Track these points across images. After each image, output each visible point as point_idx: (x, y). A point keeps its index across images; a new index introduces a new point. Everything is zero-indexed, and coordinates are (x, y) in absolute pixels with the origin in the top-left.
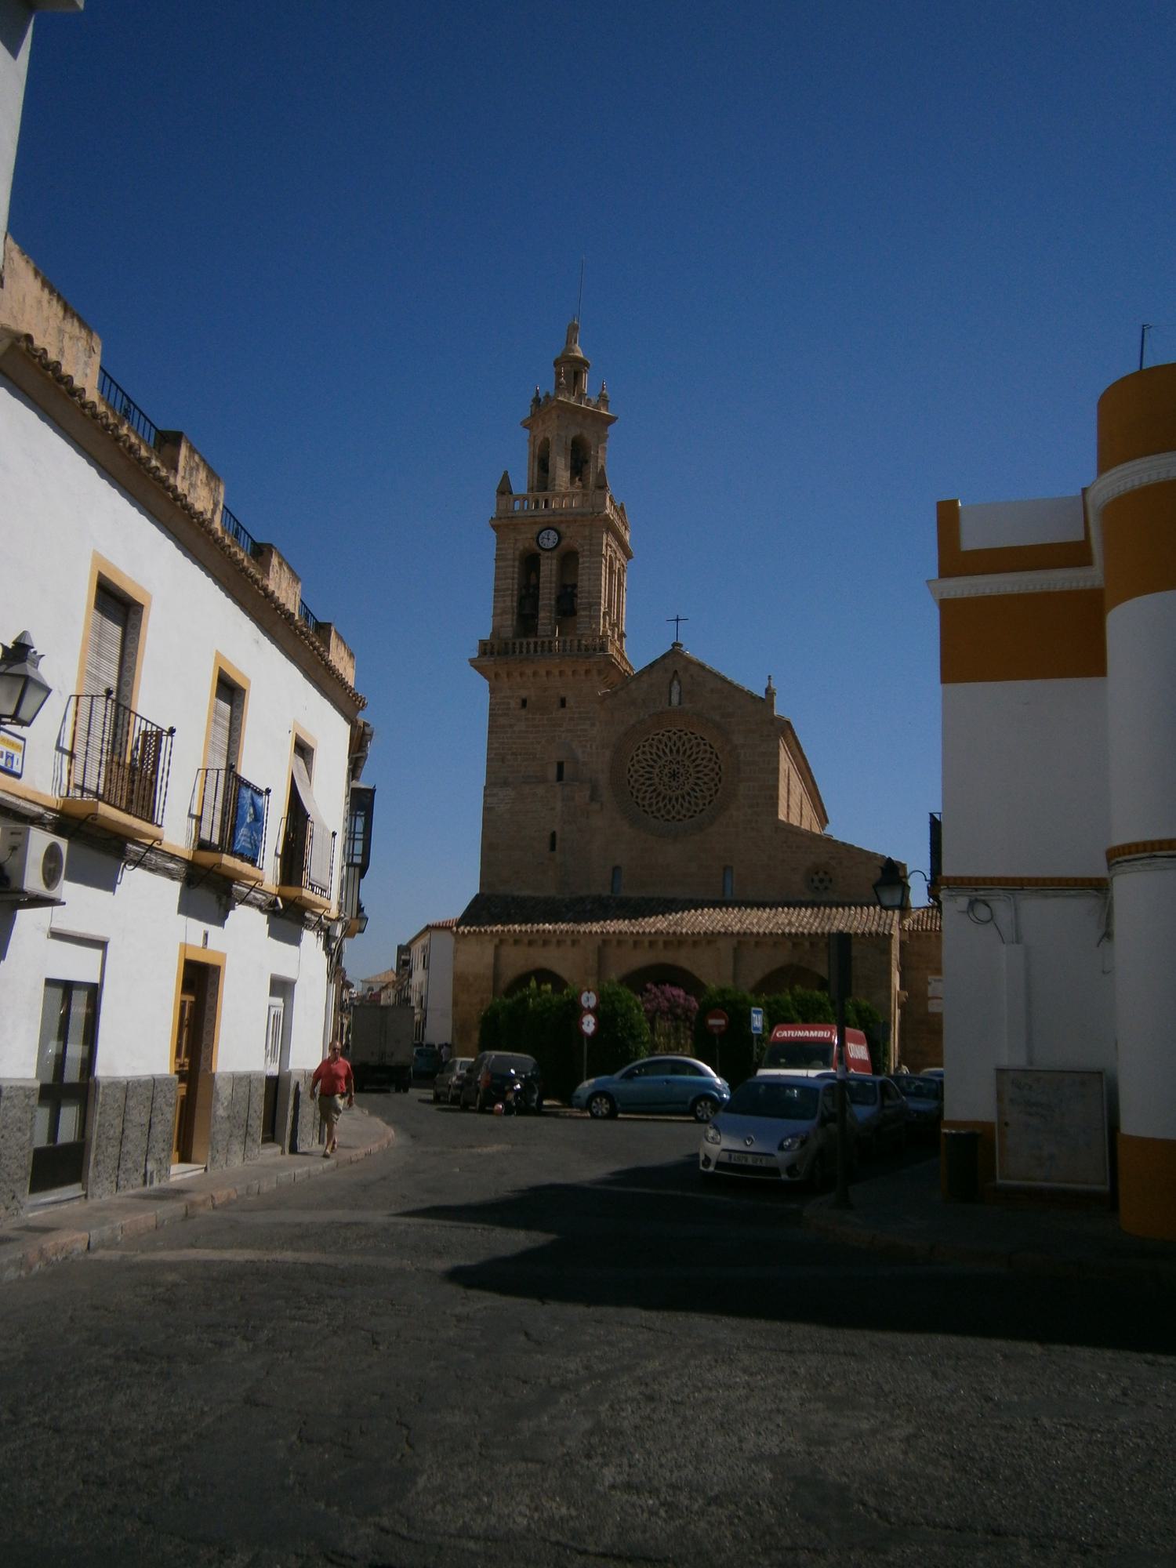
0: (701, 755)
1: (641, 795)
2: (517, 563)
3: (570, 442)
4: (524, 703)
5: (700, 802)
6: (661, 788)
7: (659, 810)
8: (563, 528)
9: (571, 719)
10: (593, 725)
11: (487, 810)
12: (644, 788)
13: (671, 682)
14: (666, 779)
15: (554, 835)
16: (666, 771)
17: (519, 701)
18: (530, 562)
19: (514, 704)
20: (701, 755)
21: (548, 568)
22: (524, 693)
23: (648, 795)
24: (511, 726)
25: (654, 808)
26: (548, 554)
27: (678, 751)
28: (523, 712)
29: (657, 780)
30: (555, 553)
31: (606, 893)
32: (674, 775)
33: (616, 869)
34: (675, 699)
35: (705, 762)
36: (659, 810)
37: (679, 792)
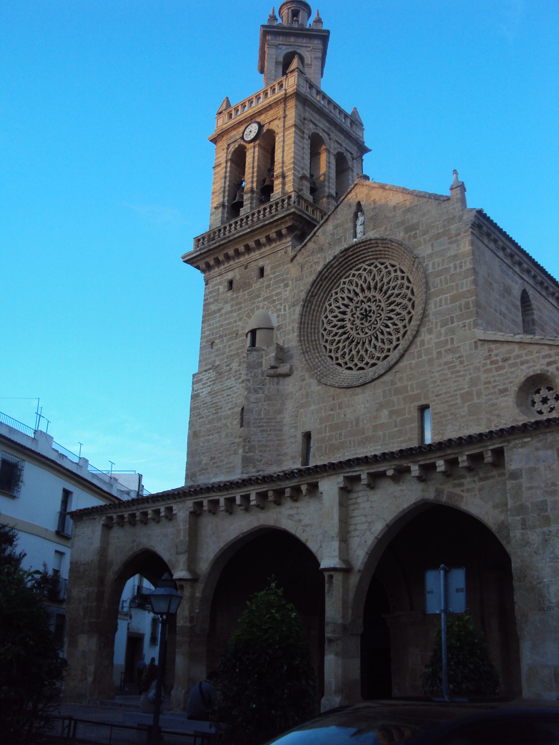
0: (392, 284)
1: (333, 347)
2: (229, 164)
3: (281, 59)
4: (231, 283)
5: (394, 337)
6: (353, 333)
7: (352, 359)
8: (260, 119)
9: (268, 286)
10: (286, 285)
11: (194, 397)
12: (337, 338)
13: (356, 217)
14: (358, 322)
15: (243, 409)
16: (358, 313)
17: (226, 284)
18: (238, 158)
19: (222, 289)
20: (392, 284)
21: (252, 157)
22: (230, 275)
23: (341, 345)
24: (220, 310)
25: (347, 357)
26: (252, 144)
27: (369, 288)
28: (230, 294)
29: (349, 326)
30: (257, 142)
31: (298, 465)
32: (366, 316)
33: (307, 436)
34: (359, 229)
35: (396, 292)
36: (352, 359)
37: (370, 333)
